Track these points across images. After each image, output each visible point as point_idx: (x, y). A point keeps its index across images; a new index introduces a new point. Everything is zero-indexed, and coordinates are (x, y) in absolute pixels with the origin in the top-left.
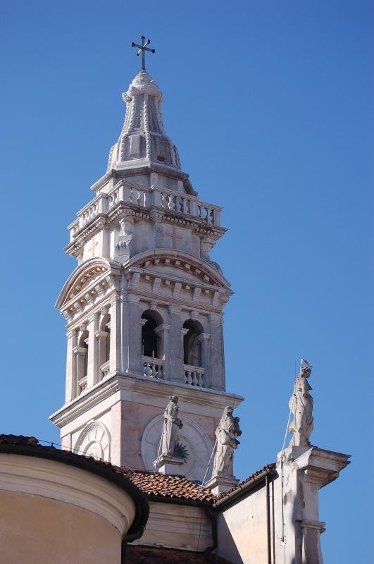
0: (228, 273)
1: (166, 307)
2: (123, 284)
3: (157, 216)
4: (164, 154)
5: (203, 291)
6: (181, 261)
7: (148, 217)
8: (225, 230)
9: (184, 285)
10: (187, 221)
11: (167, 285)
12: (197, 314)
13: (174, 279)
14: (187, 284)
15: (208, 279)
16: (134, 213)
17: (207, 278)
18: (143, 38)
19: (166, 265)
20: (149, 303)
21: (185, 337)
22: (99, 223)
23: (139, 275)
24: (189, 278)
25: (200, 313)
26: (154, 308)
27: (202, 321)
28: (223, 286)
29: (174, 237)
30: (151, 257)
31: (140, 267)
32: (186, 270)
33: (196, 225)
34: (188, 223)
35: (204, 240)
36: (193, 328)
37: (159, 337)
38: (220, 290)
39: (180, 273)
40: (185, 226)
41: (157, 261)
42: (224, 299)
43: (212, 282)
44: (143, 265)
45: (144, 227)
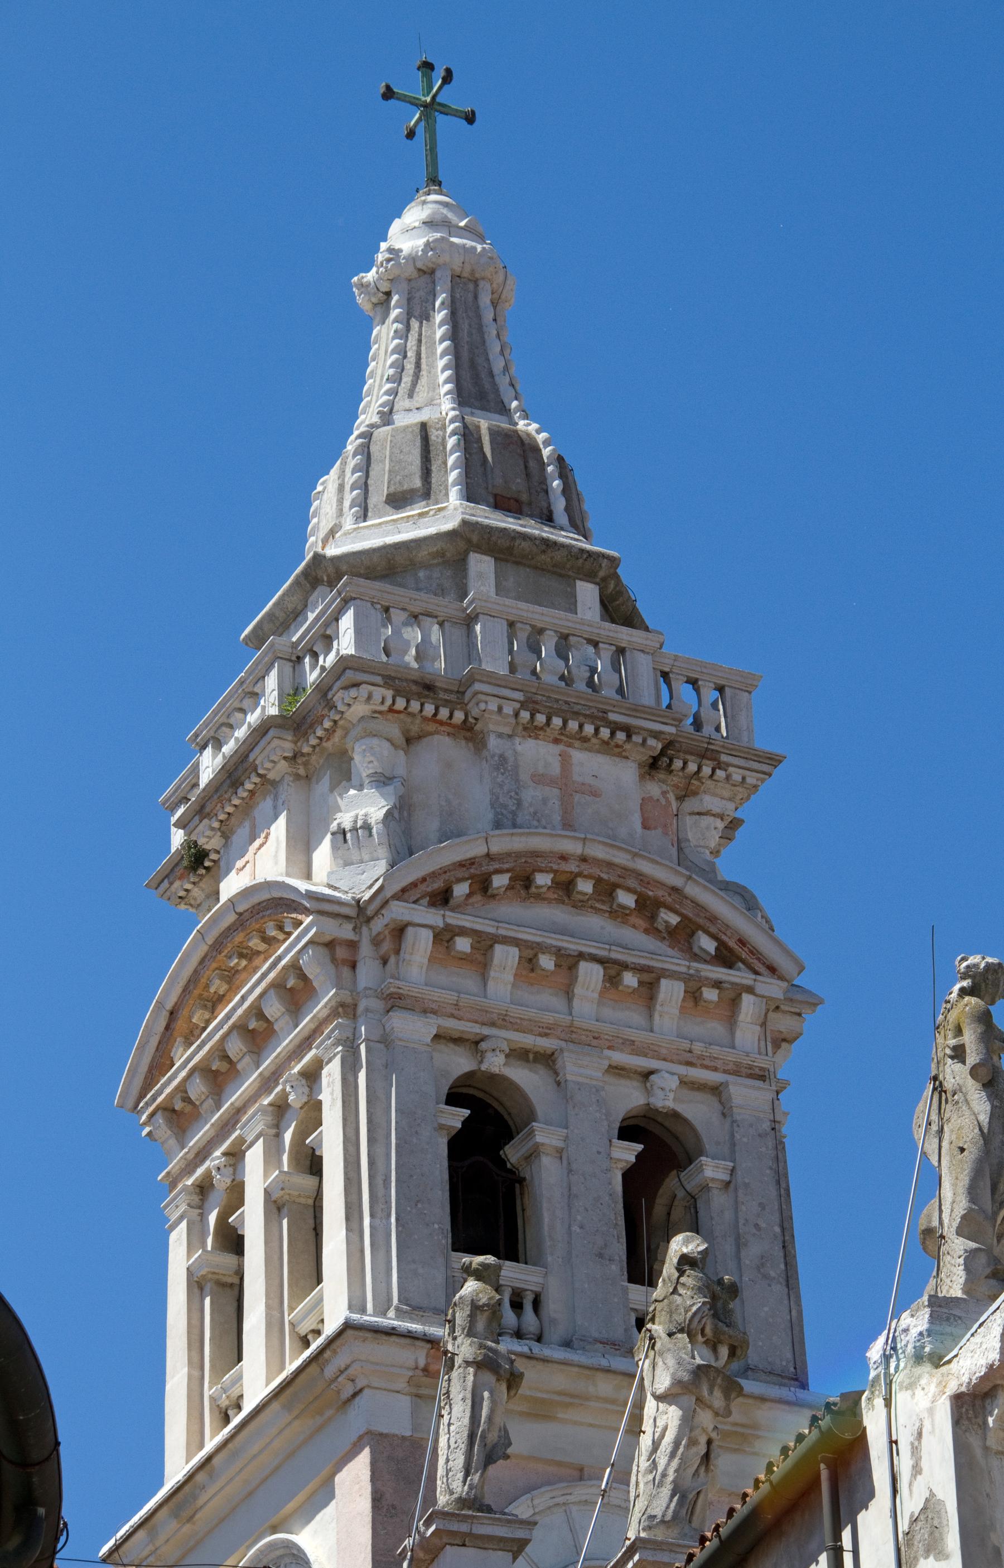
0: (794, 924)
1: (547, 1060)
2: (368, 972)
3: (495, 712)
5: (693, 996)
7: (459, 716)
8: (774, 760)
9: (613, 970)
10: (615, 728)
11: (546, 975)
12: (674, 1083)
13: (573, 946)
14: (625, 966)
15: (712, 945)
16: (401, 703)
17: (707, 944)
18: (427, 67)
19: (539, 897)
20: (475, 1044)
21: (628, 1176)
22: (274, 758)
23: (426, 937)
24: (635, 942)
25: (685, 1083)
26: (495, 1063)
27: (698, 1112)
28: (772, 970)
29: (566, 784)
30: (471, 862)
31: (432, 904)
32: (619, 914)
33: (651, 742)
34: (621, 736)
35: (691, 804)
36: (658, 1153)
37: (521, 1181)
38: (760, 988)
39: (595, 923)
40: (608, 748)
41: (500, 881)
42: (783, 1023)
43: (725, 957)
44: (442, 898)
45: (442, 750)
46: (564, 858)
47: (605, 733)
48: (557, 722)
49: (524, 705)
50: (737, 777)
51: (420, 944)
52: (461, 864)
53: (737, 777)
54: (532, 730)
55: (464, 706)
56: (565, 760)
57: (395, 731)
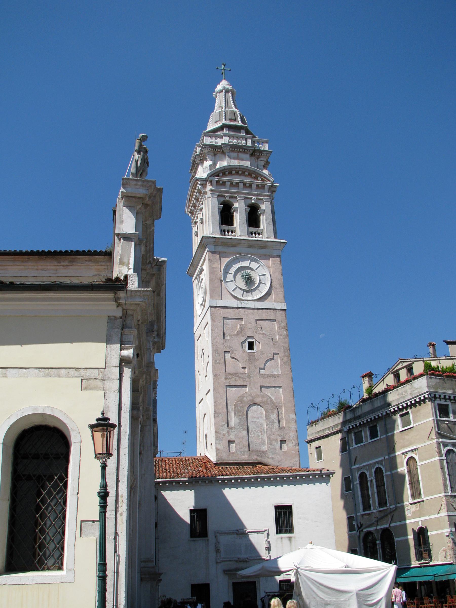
4: (233, 118)
6: (242, 171)
7: (221, 151)
9: (245, 184)
10: (245, 149)
19: (234, 175)
30: (222, 170)
32: (246, 176)
34: (246, 151)
35: (259, 159)
40: (245, 152)
41: (227, 173)
43: (262, 180)
44: (218, 176)
46: (236, 168)
47: (243, 150)
48: (236, 149)
49: (230, 148)
50: (265, 155)
51: (215, 182)
52: (220, 171)
53: (265, 155)
54: (232, 151)
55: (222, 149)
56: (238, 155)
57: (212, 154)
